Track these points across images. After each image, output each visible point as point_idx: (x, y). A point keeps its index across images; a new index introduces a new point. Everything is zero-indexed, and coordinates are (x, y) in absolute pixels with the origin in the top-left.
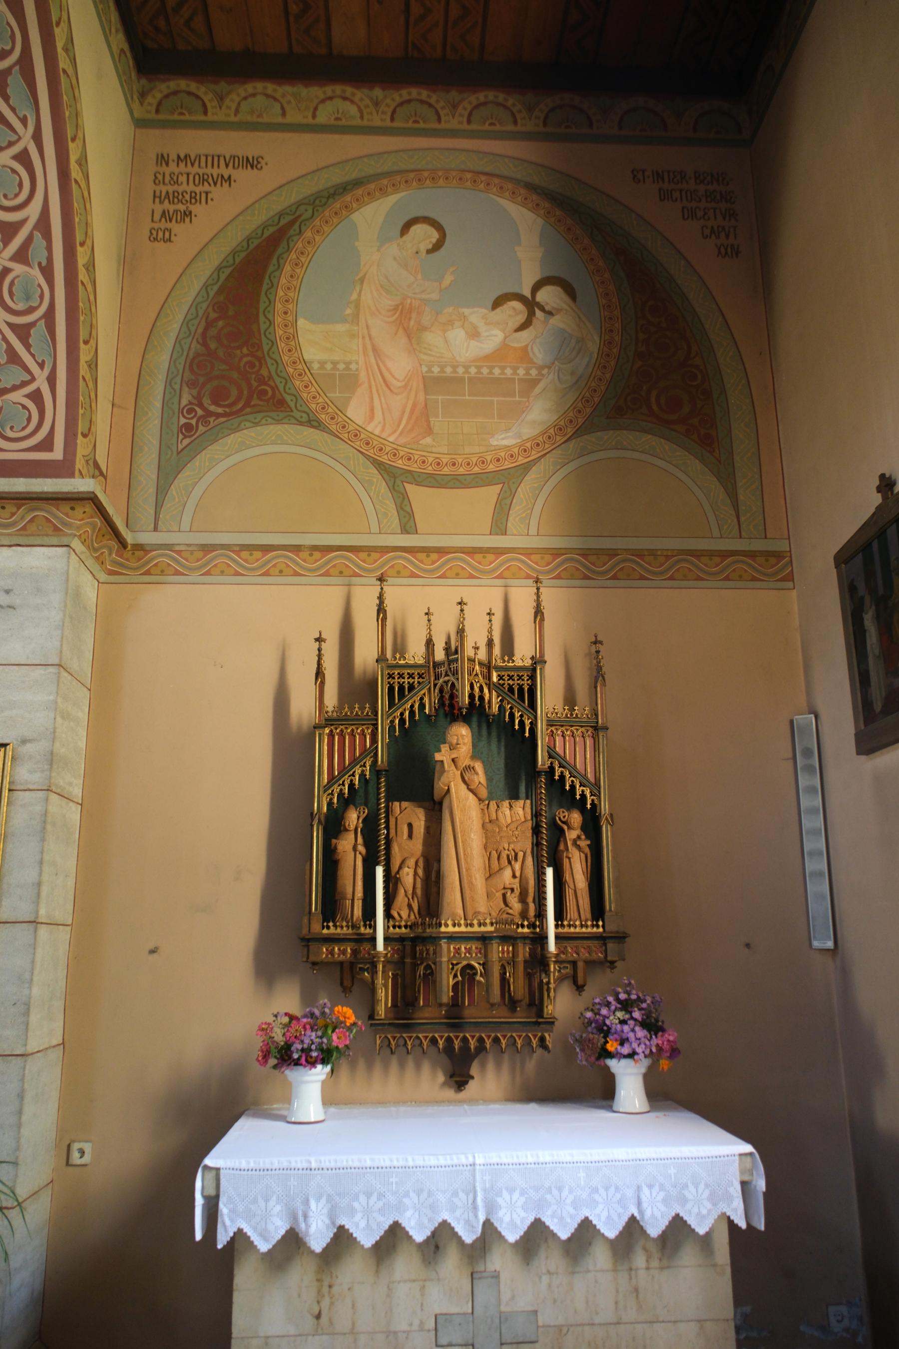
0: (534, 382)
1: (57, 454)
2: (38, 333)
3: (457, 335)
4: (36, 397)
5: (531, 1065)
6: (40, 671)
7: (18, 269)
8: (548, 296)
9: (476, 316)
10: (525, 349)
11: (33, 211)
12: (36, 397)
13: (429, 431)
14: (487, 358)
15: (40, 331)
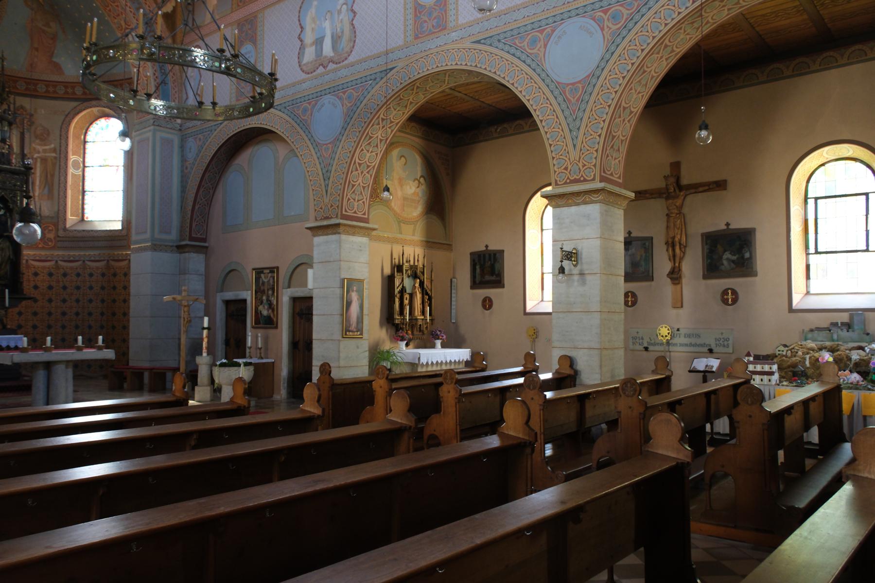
0: (419, 201)
1: (366, 216)
2: (366, 188)
3: (408, 187)
4: (364, 202)
5: (416, 343)
6: (366, 265)
7: (367, 174)
8: (422, 180)
9: (411, 182)
10: (418, 193)
11: (373, 164)
12: (364, 202)
13: (404, 211)
14: (412, 194)
15: (367, 187)
